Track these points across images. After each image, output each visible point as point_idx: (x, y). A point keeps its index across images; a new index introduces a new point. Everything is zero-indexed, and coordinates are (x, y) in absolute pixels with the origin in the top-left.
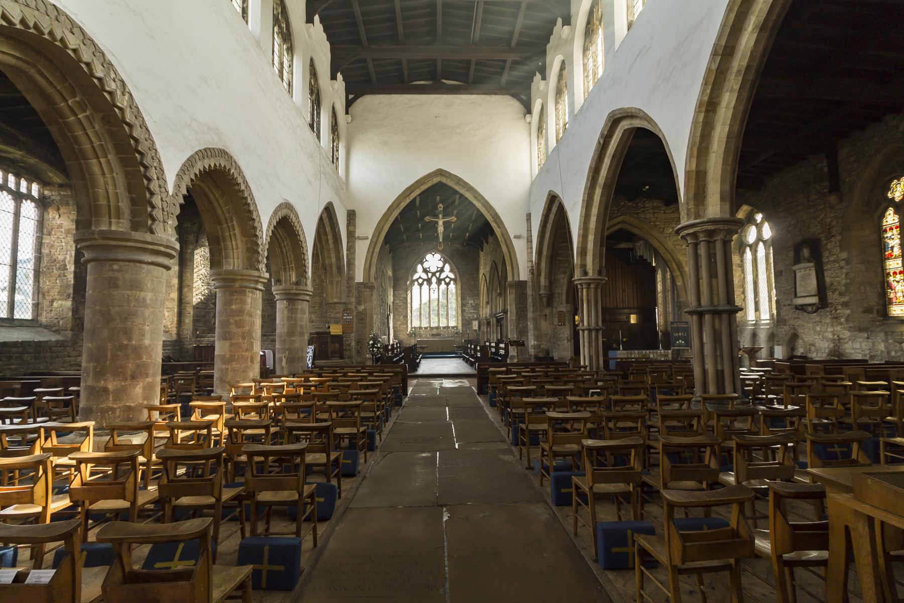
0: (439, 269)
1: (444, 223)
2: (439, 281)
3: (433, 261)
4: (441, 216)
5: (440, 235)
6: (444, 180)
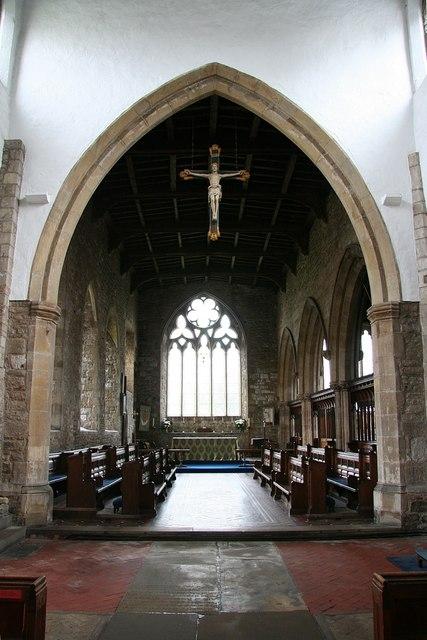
0: (212, 323)
1: (222, 182)
2: (212, 342)
3: (204, 310)
4: (215, 167)
5: (213, 206)
6: (223, 89)
